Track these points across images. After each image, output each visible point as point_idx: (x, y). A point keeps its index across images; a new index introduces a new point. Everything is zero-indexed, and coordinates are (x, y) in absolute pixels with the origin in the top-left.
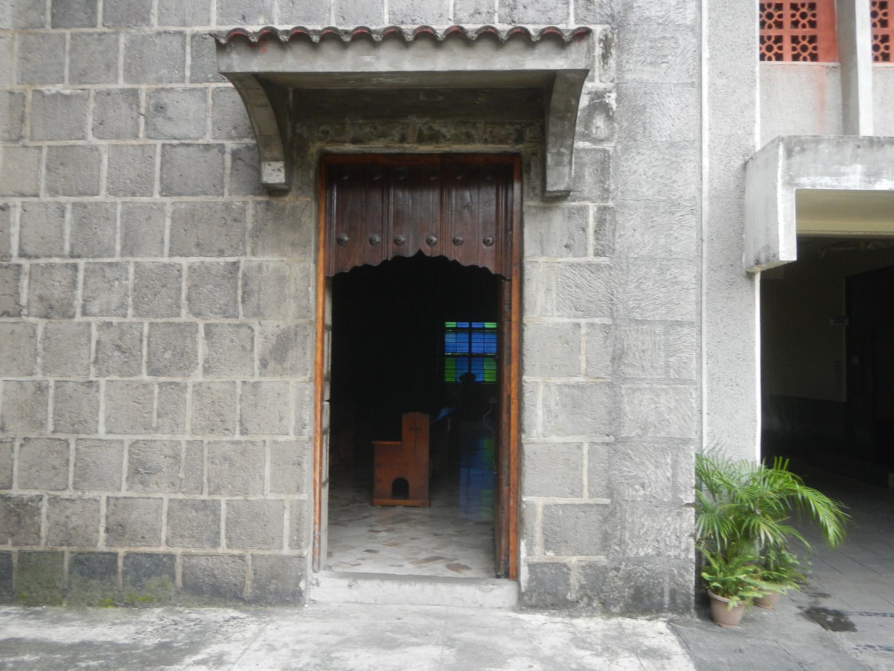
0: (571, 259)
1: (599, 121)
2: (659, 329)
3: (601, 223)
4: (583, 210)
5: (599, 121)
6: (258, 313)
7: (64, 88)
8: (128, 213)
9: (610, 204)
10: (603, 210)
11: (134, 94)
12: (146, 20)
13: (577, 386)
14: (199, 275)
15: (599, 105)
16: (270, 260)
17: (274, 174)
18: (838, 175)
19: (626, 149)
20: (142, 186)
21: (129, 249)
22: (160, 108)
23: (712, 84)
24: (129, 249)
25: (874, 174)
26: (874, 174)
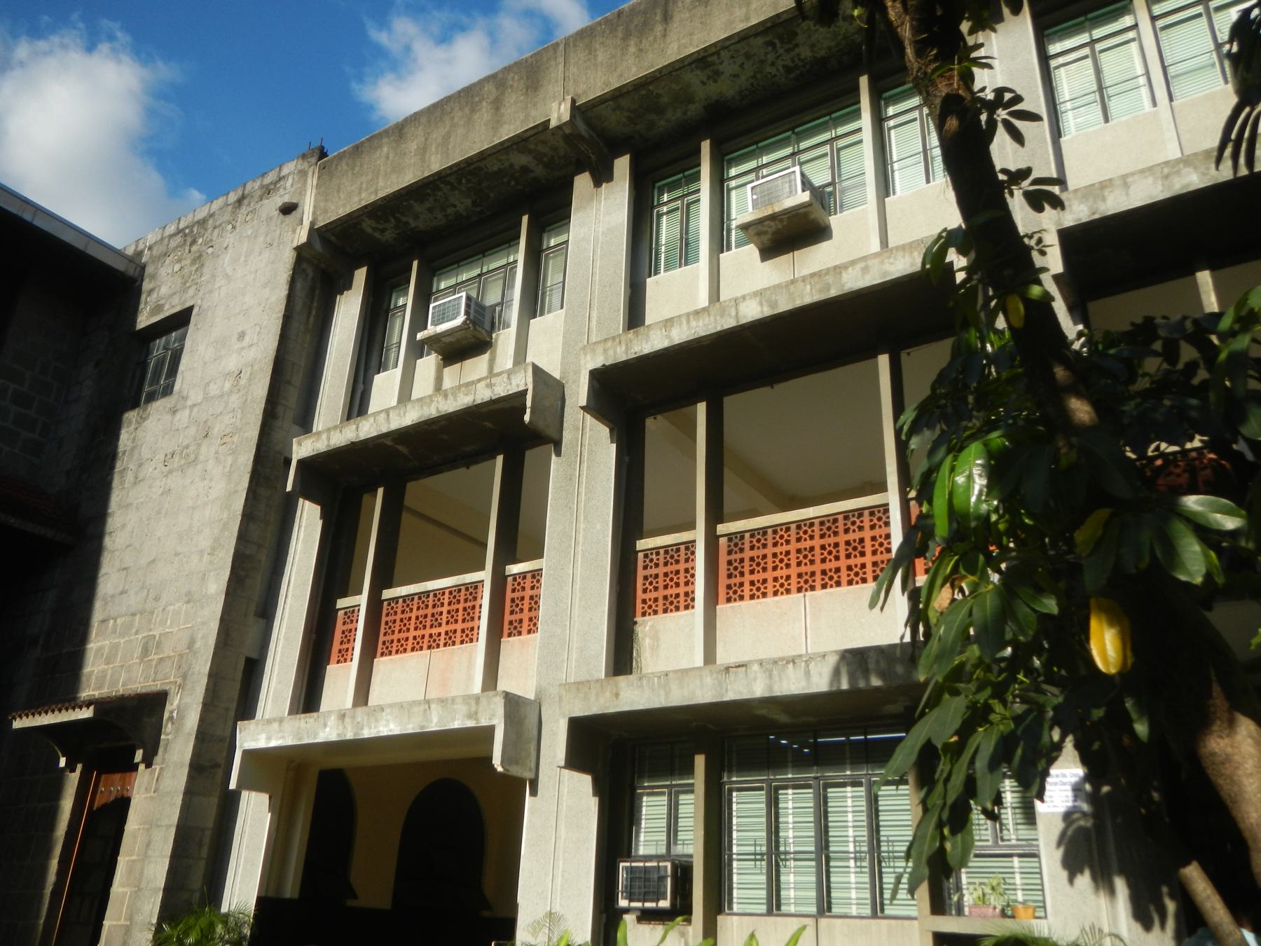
0: (146, 795)
2: (164, 829)
4: (156, 769)
9: (163, 766)
10: (161, 769)
13: (134, 861)
15: (171, 718)
18: (257, 740)
19: (175, 737)
23: (275, 689)
26: (269, 739)
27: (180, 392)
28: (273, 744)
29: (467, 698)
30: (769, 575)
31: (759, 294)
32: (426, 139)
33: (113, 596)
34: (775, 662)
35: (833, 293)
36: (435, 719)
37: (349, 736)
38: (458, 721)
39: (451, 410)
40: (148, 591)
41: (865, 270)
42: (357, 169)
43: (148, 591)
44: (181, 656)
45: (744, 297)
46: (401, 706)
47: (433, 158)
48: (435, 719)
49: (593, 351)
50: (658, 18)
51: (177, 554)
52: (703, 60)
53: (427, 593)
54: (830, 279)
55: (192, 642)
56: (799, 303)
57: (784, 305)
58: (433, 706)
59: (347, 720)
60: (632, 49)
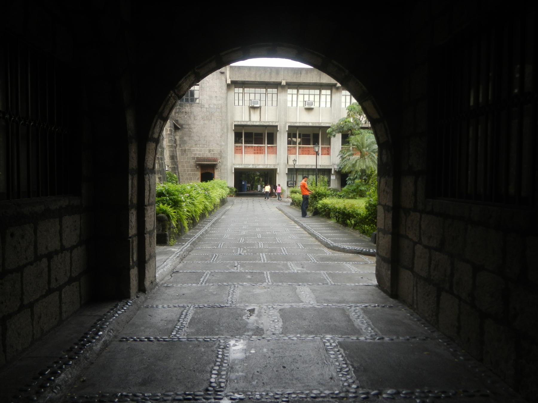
1: (220, 163)
3: (220, 170)
5: (220, 163)
6: (197, 176)
7: (182, 160)
8: (187, 169)
11: (187, 161)
12: (188, 155)
14: (192, 173)
15: (220, 162)
16: (197, 173)
17: (198, 167)
20: (188, 167)
21: (188, 172)
22: (189, 162)
24: (188, 172)
25: (239, 166)
26: (239, 166)
27: (201, 104)
28: (240, 167)
29: (273, 165)
30: (304, 152)
31: (311, 123)
32: (256, 73)
33: (197, 141)
34: (312, 165)
35: (320, 125)
36: (268, 167)
37: (254, 167)
38: (272, 167)
39: (265, 124)
40: (206, 141)
41: (324, 124)
42: (240, 72)
43: (206, 141)
44: (219, 153)
45: (310, 123)
46: (263, 165)
47: (258, 78)
48: (268, 167)
49: (289, 123)
50: (300, 73)
51: (212, 136)
52: (305, 83)
53: (252, 146)
54: (320, 124)
55: (221, 152)
56: (316, 125)
57: (314, 125)
58: (268, 165)
59: (254, 165)
60: (295, 76)
